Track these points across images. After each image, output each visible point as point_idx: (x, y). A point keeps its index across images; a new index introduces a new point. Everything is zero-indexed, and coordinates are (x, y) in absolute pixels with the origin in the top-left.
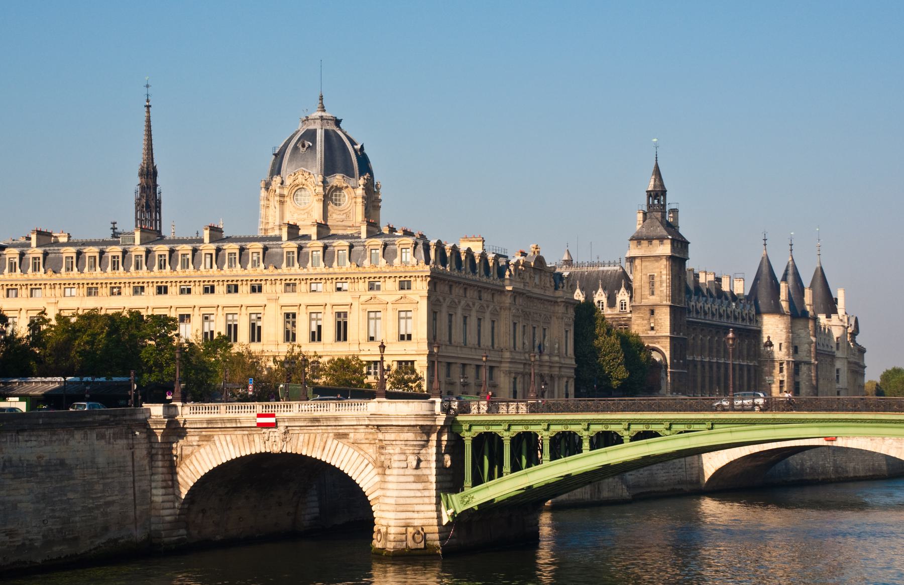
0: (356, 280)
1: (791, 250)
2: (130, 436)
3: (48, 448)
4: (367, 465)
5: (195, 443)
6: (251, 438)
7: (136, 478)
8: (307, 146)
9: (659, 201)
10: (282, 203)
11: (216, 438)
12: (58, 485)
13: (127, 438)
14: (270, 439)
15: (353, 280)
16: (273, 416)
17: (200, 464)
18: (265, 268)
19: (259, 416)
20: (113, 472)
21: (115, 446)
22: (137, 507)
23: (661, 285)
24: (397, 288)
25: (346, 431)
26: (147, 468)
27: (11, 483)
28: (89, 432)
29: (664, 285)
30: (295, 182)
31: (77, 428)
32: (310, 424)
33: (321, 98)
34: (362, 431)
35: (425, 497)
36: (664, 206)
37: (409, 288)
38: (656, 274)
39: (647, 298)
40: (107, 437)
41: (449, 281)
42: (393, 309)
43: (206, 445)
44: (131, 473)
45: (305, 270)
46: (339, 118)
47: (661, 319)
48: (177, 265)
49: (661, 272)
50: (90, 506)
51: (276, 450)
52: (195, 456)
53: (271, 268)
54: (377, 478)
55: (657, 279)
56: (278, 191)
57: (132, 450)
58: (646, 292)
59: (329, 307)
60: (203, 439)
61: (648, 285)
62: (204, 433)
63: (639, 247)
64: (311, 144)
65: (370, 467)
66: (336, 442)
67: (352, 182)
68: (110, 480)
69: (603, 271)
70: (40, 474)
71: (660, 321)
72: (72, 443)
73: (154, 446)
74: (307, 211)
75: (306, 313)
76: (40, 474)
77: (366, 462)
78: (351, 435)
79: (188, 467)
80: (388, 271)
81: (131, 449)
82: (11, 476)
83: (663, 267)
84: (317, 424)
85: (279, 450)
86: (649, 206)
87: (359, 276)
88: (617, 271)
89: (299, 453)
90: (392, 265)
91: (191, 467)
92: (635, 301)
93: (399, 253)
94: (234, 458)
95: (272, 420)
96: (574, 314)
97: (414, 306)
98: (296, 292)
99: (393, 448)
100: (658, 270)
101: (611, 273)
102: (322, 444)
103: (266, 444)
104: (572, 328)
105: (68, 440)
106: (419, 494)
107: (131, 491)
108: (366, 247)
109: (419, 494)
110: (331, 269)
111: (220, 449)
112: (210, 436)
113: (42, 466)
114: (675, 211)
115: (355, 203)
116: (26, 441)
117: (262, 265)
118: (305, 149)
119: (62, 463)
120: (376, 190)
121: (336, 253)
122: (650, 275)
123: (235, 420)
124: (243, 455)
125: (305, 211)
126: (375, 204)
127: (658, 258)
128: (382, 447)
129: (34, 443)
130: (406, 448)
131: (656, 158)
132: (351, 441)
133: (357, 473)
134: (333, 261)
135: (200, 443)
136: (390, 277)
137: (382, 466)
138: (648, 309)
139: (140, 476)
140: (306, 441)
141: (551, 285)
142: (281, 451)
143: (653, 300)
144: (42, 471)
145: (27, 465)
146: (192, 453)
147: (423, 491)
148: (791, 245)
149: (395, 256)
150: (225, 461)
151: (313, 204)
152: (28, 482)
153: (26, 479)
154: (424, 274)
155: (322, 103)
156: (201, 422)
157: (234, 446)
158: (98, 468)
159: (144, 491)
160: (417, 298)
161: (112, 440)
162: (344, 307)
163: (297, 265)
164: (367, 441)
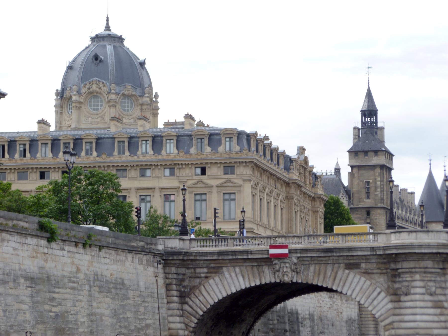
0: (184, 166)
1: (445, 170)
2: (156, 264)
3: (115, 267)
4: (379, 294)
5: (203, 275)
6: (260, 269)
7: (160, 305)
8: (99, 59)
9: (370, 120)
10: (79, 108)
11: (225, 269)
12: (122, 303)
13: (154, 267)
14: (281, 270)
15: (180, 166)
16: (285, 247)
17: (209, 294)
18: (97, 156)
19: (272, 247)
20: (148, 296)
21: (148, 272)
22: (162, 332)
23: (376, 190)
24: (222, 173)
25: (357, 261)
26: (165, 297)
27: (98, 296)
28: (134, 256)
29: (379, 190)
30: (90, 91)
31: (130, 251)
32: (322, 255)
33: (108, 20)
34: (374, 261)
35: (441, 321)
36: (376, 123)
37: (233, 173)
38: (371, 181)
39: (363, 201)
40: (144, 263)
41: (262, 168)
42: (218, 192)
43: (215, 276)
44: (157, 300)
45: (136, 157)
46: (123, 37)
47: (376, 219)
48: (15, 153)
49: (376, 179)
50: (139, 326)
51: (287, 279)
52: (204, 287)
53: (104, 156)
54: (390, 305)
55: (372, 185)
56: (74, 98)
57: (157, 278)
58: (363, 196)
59: (157, 191)
60: (212, 270)
61: (364, 190)
62: (212, 265)
63: (357, 158)
64: (103, 58)
65: (383, 295)
66: (347, 271)
67: (138, 92)
68: (147, 304)
69: (326, 179)
70: (113, 290)
71: (375, 221)
72: (127, 264)
73: (168, 277)
74: (100, 115)
75: (137, 196)
76: (113, 290)
77: (378, 290)
78: (363, 265)
79: (197, 297)
80: (213, 157)
81: (156, 277)
82: (97, 289)
83: (377, 174)
84: (330, 254)
85: (290, 279)
86: (362, 123)
87: (187, 163)
88: (333, 179)
89: (310, 282)
90: (217, 152)
91: (201, 298)
92: (353, 204)
93: (223, 142)
94: (243, 287)
95: (285, 251)
96: (324, 209)
97: (238, 189)
98: (126, 177)
99: (412, 275)
100: (373, 177)
101: (329, 181)
102: (333, 274)
103: (276, 275)
104: (323, 221)
105: (125, 261)
106: (436, 318)
107: (157, 317)
108: (193, 137)
109: (436, 318)
110: (160, 157)
111: (229, 280)
112: (219, 268)
113: (113, 283)
114: (382, 129)
115: (141, 109)
116: (104, 257)
117: (95, 153)
118: (98, 61)
119: (123, 283)
120: (154, 99)
121: (164, 142)
122: (366, 182)
123: (247, 252)
124: (253, 285)
125: (98, 116)
126: (155, 112)
127: (373, 167)
128: (394, 276)
129: (107, 261)
130: (424, 275)
131: (369, 83)
132: (363, 271)
133: (370, 300)
134: (161, 149)
135: (208, 275)
136: (216, 163)
137: (395, 294)
138: (364, 210)
139: (162, 303)
140: (317, 271)
141: (310, 183)
142: (292, 281)
143: (368, 203)
144: (113, 288)
145: (106, 280)
146: (200, 284)
147: (440, 317)
148: (445, 166)
149: (220, 144)
150: (234, 291)
151: (106, 110)
152: (107, 297)
153: (105, 294)
154: (247, 161)
155: (107, 24)
156: (212, 254)
157: (243, 277)
158: (141, 292)
159: (164, 318)
160: (239, 182)
161: (146, 267)
162: (172, 190)
163: (127, 153)
164: (379, 271)
